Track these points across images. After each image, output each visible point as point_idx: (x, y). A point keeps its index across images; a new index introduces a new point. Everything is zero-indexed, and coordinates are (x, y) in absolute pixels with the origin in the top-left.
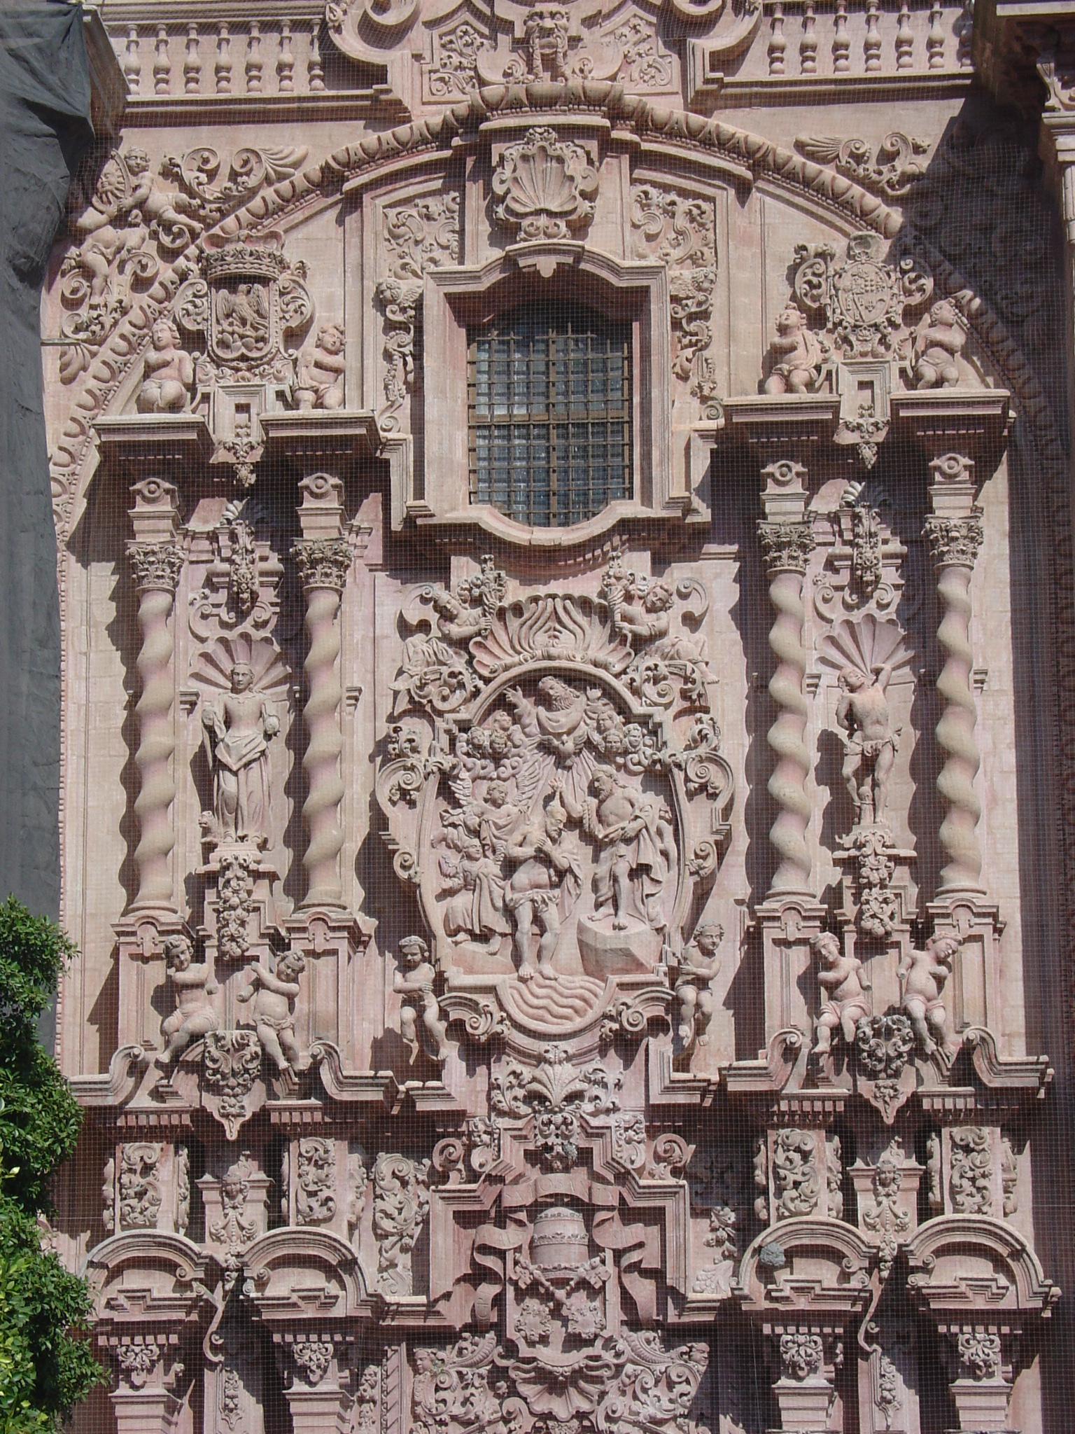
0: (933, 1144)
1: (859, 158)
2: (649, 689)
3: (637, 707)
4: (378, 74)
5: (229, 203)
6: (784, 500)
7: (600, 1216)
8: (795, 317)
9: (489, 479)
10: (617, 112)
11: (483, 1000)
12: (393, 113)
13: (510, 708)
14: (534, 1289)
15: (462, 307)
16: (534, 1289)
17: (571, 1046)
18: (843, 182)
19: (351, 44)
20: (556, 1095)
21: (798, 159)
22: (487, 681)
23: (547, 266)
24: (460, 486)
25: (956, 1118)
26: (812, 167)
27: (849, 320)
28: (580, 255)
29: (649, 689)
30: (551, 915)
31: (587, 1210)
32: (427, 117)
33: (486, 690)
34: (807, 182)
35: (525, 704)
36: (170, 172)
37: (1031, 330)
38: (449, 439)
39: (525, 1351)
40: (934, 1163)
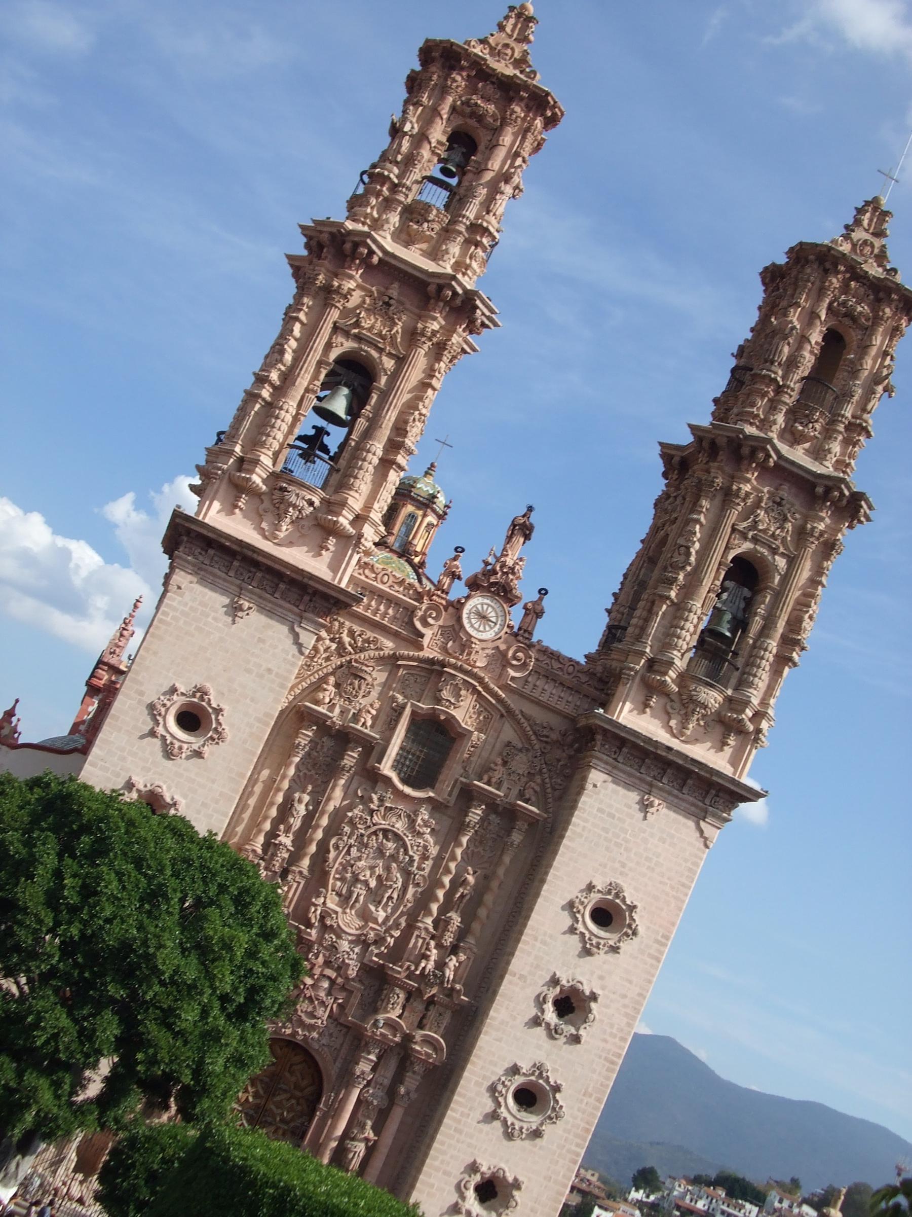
0: (431, 1008)
1: (536, 724)
2: (415, 848)
3: (411, 853)
4: (422, 636)
5: (362, 650)
6: (476, 814)
7: (336, 987)
8: (499, 761)
9: (398, 765)
10: (480, 680)
11: (334, 916)
12: (421, 648)
13: (377, 835)
14: (310, 999)
15: (413, 713)
16: (310, 999)
17: (350, 938)
18: (528, 729)
19: (418, 625)
20: (341, 949)
21: (520, 716)
22: (374, 825)
23: (442, 717)
24: (390, 763)
25: (441, 1005)
26: (523, 720)
27: (513, 769)
28: (453, 717)
29: (415, 848)
30: (362, 898)
31: (332, 982)
32: (427, 653)
33: (373, 829)
34: (518, 722)
35: (381, 836)
36: (351, 633)
37: (557, 793)
38: (393, 750)
39: (299, 1013)
40: (429, 1013)
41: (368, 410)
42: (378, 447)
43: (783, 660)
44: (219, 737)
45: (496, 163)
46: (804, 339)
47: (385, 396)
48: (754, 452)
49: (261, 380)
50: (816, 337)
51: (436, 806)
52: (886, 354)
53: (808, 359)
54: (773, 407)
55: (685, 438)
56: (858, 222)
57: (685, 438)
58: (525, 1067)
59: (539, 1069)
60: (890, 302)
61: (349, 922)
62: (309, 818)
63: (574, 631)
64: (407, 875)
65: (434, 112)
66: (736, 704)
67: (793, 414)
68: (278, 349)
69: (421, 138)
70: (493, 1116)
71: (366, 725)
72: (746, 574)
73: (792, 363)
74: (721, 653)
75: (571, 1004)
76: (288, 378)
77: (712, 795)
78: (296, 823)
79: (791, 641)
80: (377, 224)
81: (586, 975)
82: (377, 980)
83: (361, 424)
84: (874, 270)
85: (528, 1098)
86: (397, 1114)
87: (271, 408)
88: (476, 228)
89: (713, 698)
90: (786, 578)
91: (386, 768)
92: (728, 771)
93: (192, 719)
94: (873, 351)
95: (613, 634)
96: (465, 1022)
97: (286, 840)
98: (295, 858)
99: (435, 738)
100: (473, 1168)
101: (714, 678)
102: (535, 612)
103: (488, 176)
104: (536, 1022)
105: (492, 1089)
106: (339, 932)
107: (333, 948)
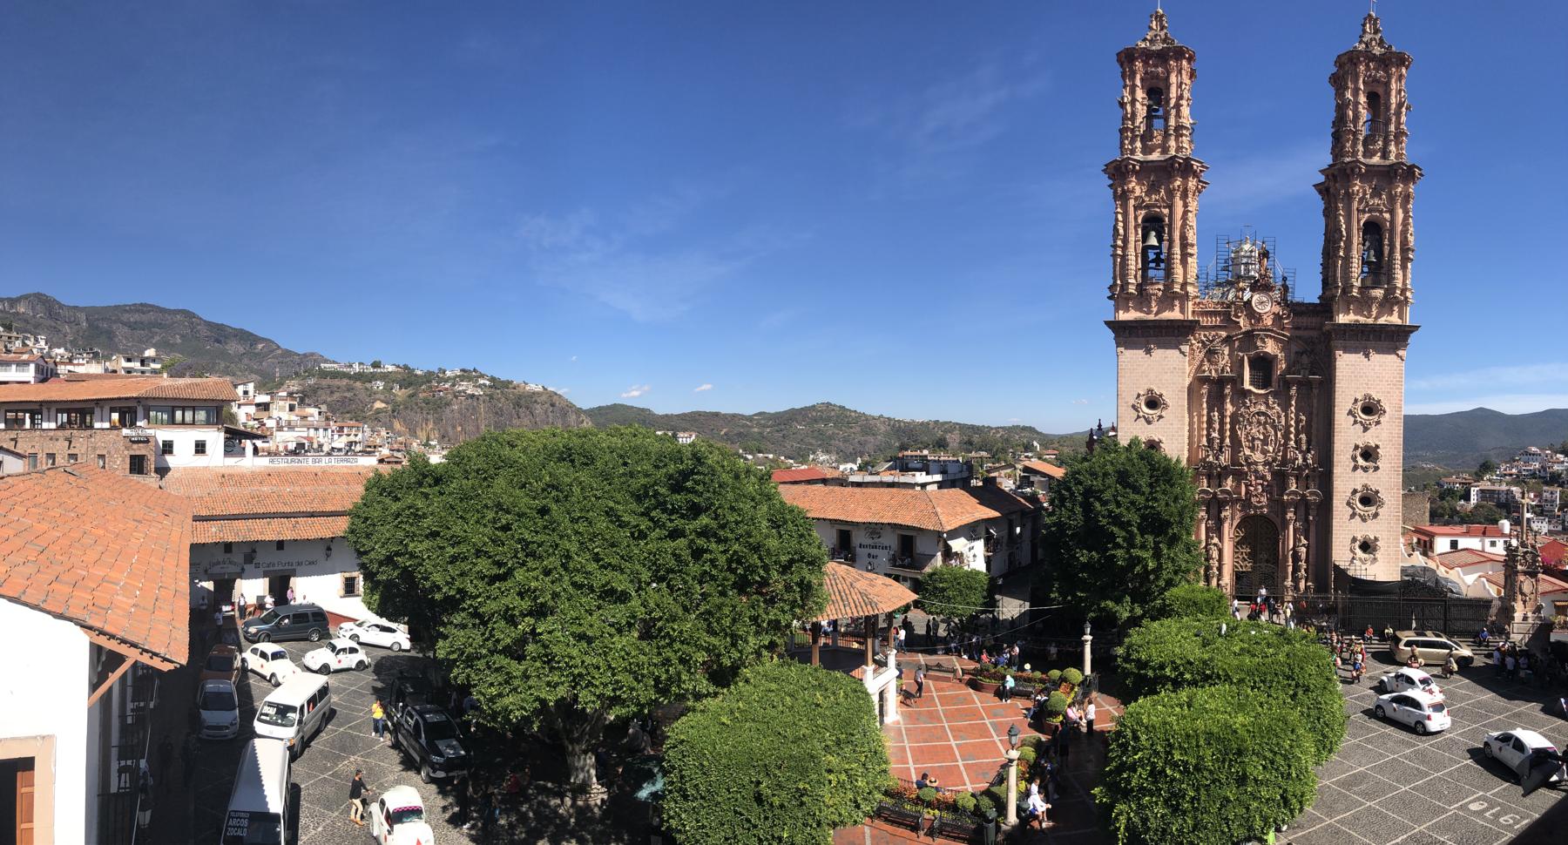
9: (1252, 383)
41: (1166, 237)
42: (1177, 250)
43: (1405, 260)
44: (1166, 406)
45: (1173, 93)
46: (1357, 103)
47: (1170, 226)
48: (1352, 170)
49: (1115, 247)
50: (1362, 99)
51: (1275, 395)
52: (1399, 92)
53: (1364, 114)
54: (1354, 145)
55: (1322, 178)
56: (1364, 31)
57: (1322, 178)
58: (1359, 488)
59: (1365, 486)
60: (1392, 64)
61: (1258, 457)
62: (1222, 423)
63: (1308, 291)
64: (1275, 428)
65: (1133, 87)
66: (1390, 291)
67: (1365, 143)
68: (1116, 229)
69: (1134, 101)
70: (1353, 516)
71: (1228, 372)
72: (1374, 230)
73: (1356, 117)
74: (1378, 270)
75: (1369, 454)
76: (1125, 241)
77: (1393, 339)
78: (1217, 426)
79: (1405, 249)
80: (1133, 152)
81: (1370, 439)
82: (1280, 478)
83: (1165, 244)
84: (1377, 51)
85: (1367, 500)
86: (1312, 529)
87: (1124, 257)
88: (1179, 128)
89: (1378, 293)
90: (1392, 222)
91: (1247, 386)
92: (1399, 322)
93: (1153, 403)
94: (1393, 93)
95: (1325, 283)
96: (1324, 476)
97: (1215, 435)
98: (1222, 440)
99: (1263, 365)
100: (1354, 540)
101: (1376, 285)
102: (1285, 288)
103: (1173, 102)
104: (1355, 468)
105: (1348, 504)
106: (1256, 463)
107: (1256, 471)
